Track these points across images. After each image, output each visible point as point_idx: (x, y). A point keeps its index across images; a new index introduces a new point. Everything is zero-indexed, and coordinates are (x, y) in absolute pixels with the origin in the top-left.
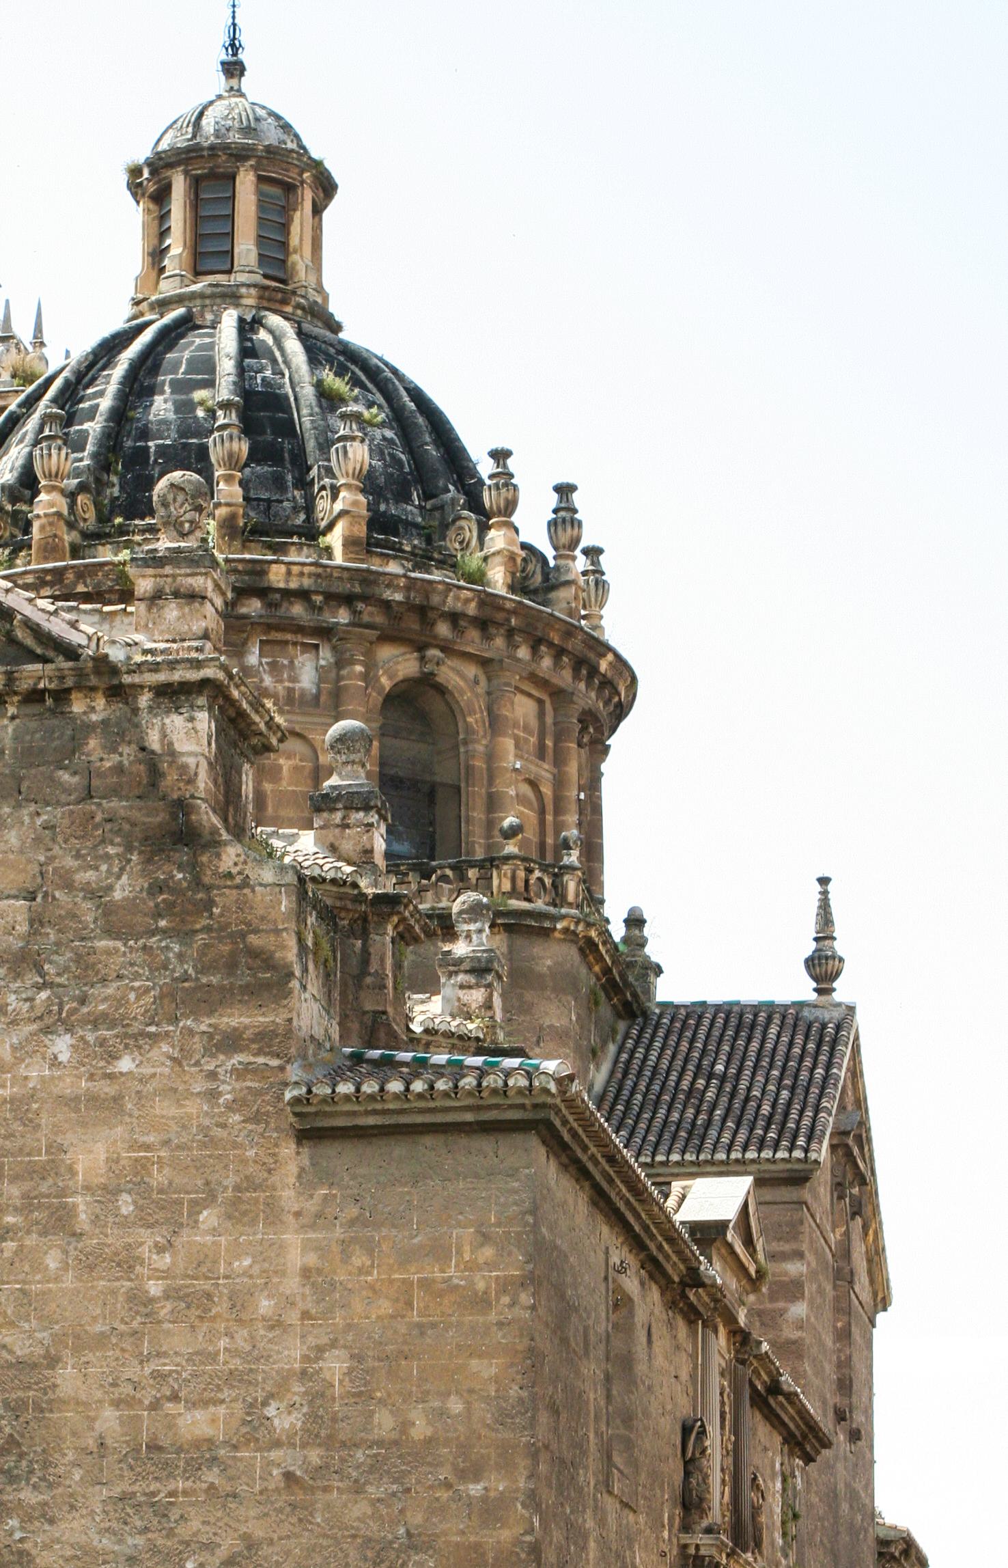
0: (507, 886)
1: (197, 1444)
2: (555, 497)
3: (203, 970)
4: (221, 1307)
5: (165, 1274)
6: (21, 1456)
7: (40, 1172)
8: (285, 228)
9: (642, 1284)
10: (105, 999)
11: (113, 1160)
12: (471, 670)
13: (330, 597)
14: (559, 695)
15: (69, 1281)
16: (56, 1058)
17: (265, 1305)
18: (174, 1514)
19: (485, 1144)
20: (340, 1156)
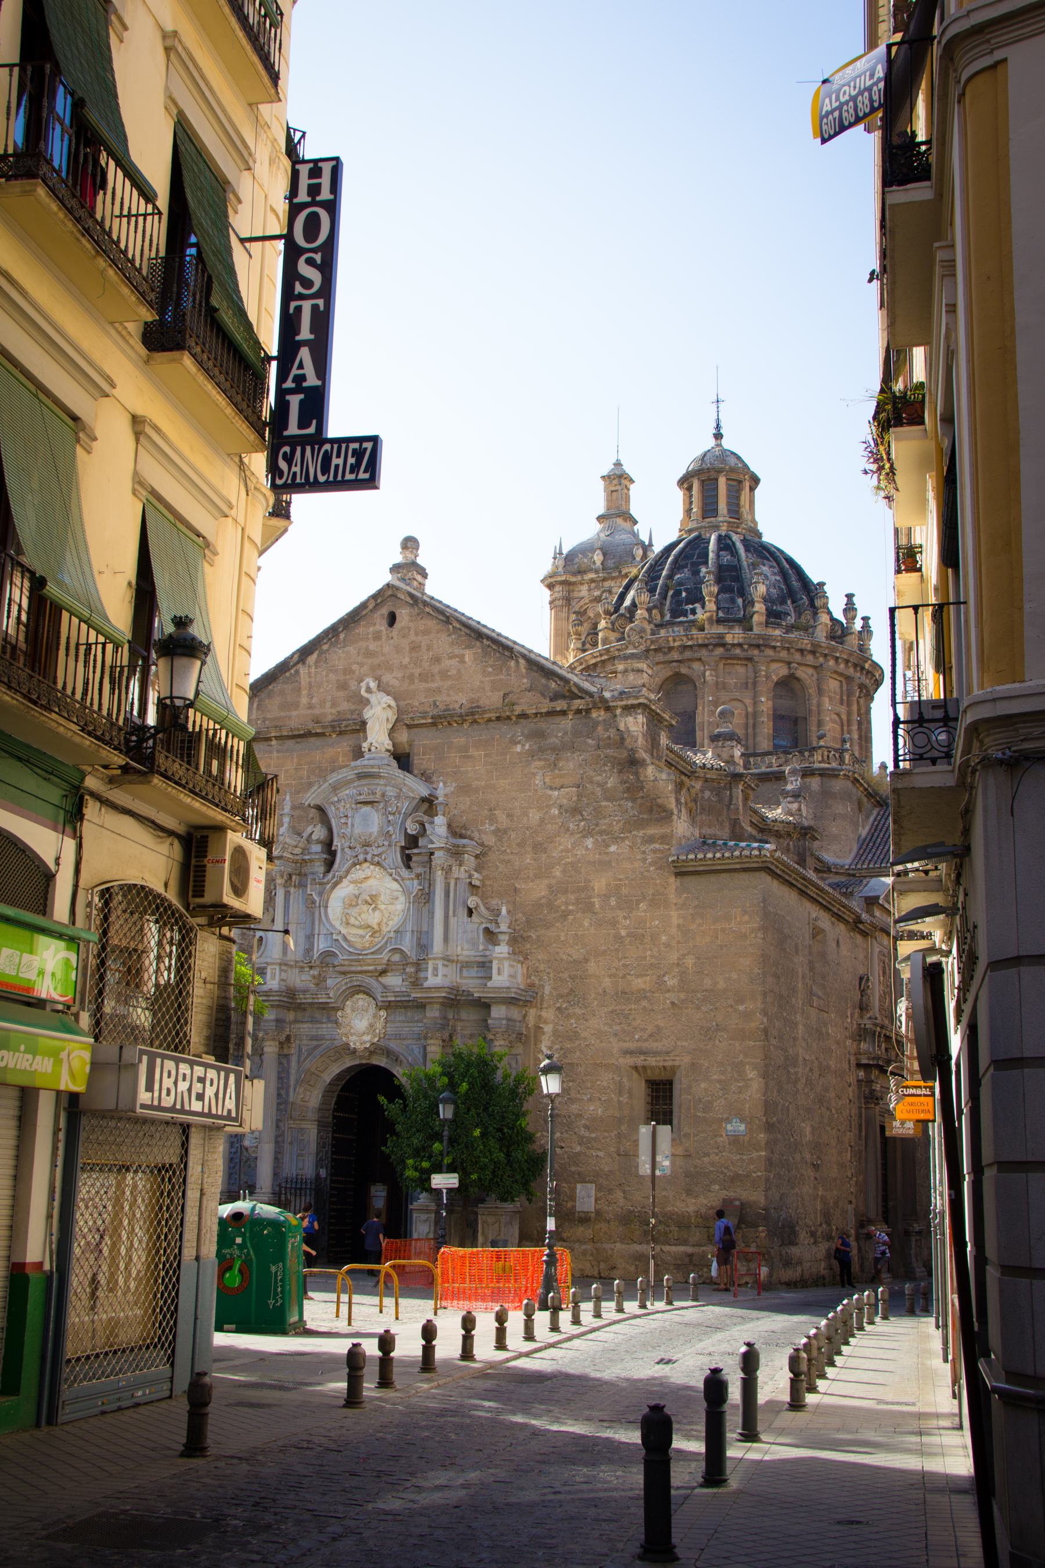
0: (820, 759)
1: (639, 991)
2: (846, 599)
3: (640, 813)
4: (647, 940)
5: (627, 928)
6: (575, 996)
8: (738, 498)
9: (833, 923)
11: (608, 885)
12: (810, 671)
13: (750, 645)
14: (849, 679)
15: (592, 931)
17: (664, 938)
18: (631, 1018)
19: (745, 876)
20: (691, 881)
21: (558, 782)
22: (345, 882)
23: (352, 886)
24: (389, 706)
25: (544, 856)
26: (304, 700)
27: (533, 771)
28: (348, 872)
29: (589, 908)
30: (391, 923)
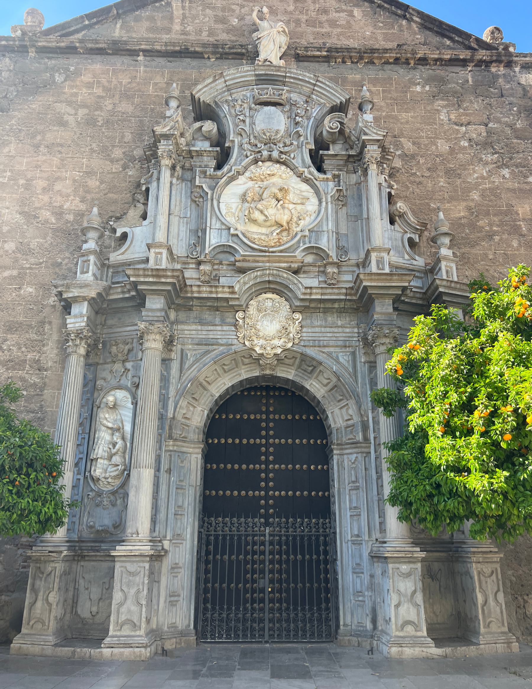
7: (506, 213)
10: (520, 158)
16: (504, 176)
21: (464, 119)
22: (242, 179)
23: (250, 184)
24: (284, 31)
25: (459, 181)
26: (177, 27)
27: (436, 108)
28: (246, 168)
29: (515, 230)
30: (302, 223)
